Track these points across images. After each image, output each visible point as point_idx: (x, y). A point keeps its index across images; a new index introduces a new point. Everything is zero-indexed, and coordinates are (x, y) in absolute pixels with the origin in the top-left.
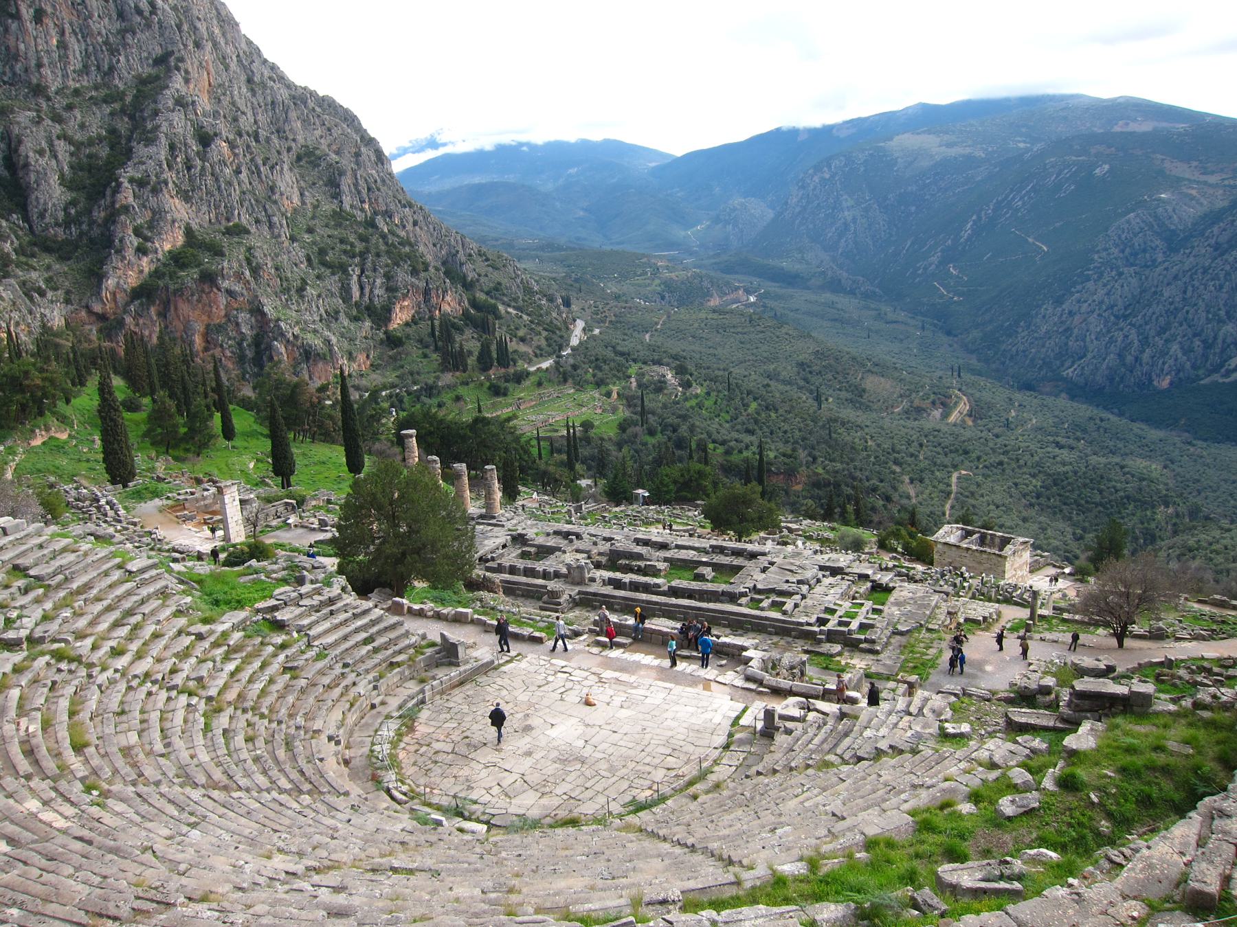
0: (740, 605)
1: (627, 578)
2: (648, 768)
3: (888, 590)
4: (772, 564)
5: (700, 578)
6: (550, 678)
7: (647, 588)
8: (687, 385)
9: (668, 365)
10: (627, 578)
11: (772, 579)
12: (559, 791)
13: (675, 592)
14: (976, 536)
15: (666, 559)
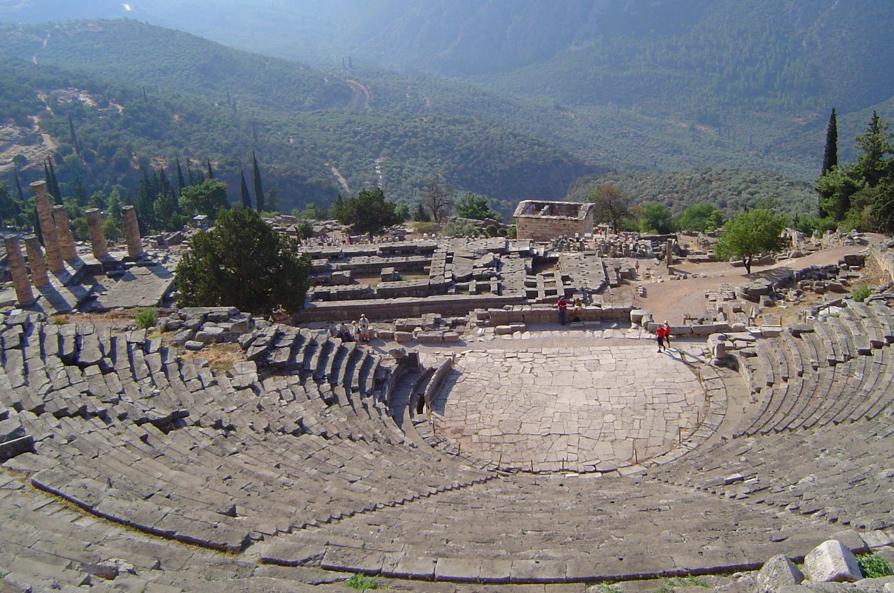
0: (451, 294)
1: (333, 290)
2: (667, 406)
3: (556, 260)
4: (452, 254)
5: (385, 278)
6: (507, 364)
7: (355, 295)
8: (106, 104)
9: (76, 86)
10: (333, 290)
11: (461, 269)
12: (621, 434)
13: (384, 294)
14: (546, 207)
15: (343, 268)
